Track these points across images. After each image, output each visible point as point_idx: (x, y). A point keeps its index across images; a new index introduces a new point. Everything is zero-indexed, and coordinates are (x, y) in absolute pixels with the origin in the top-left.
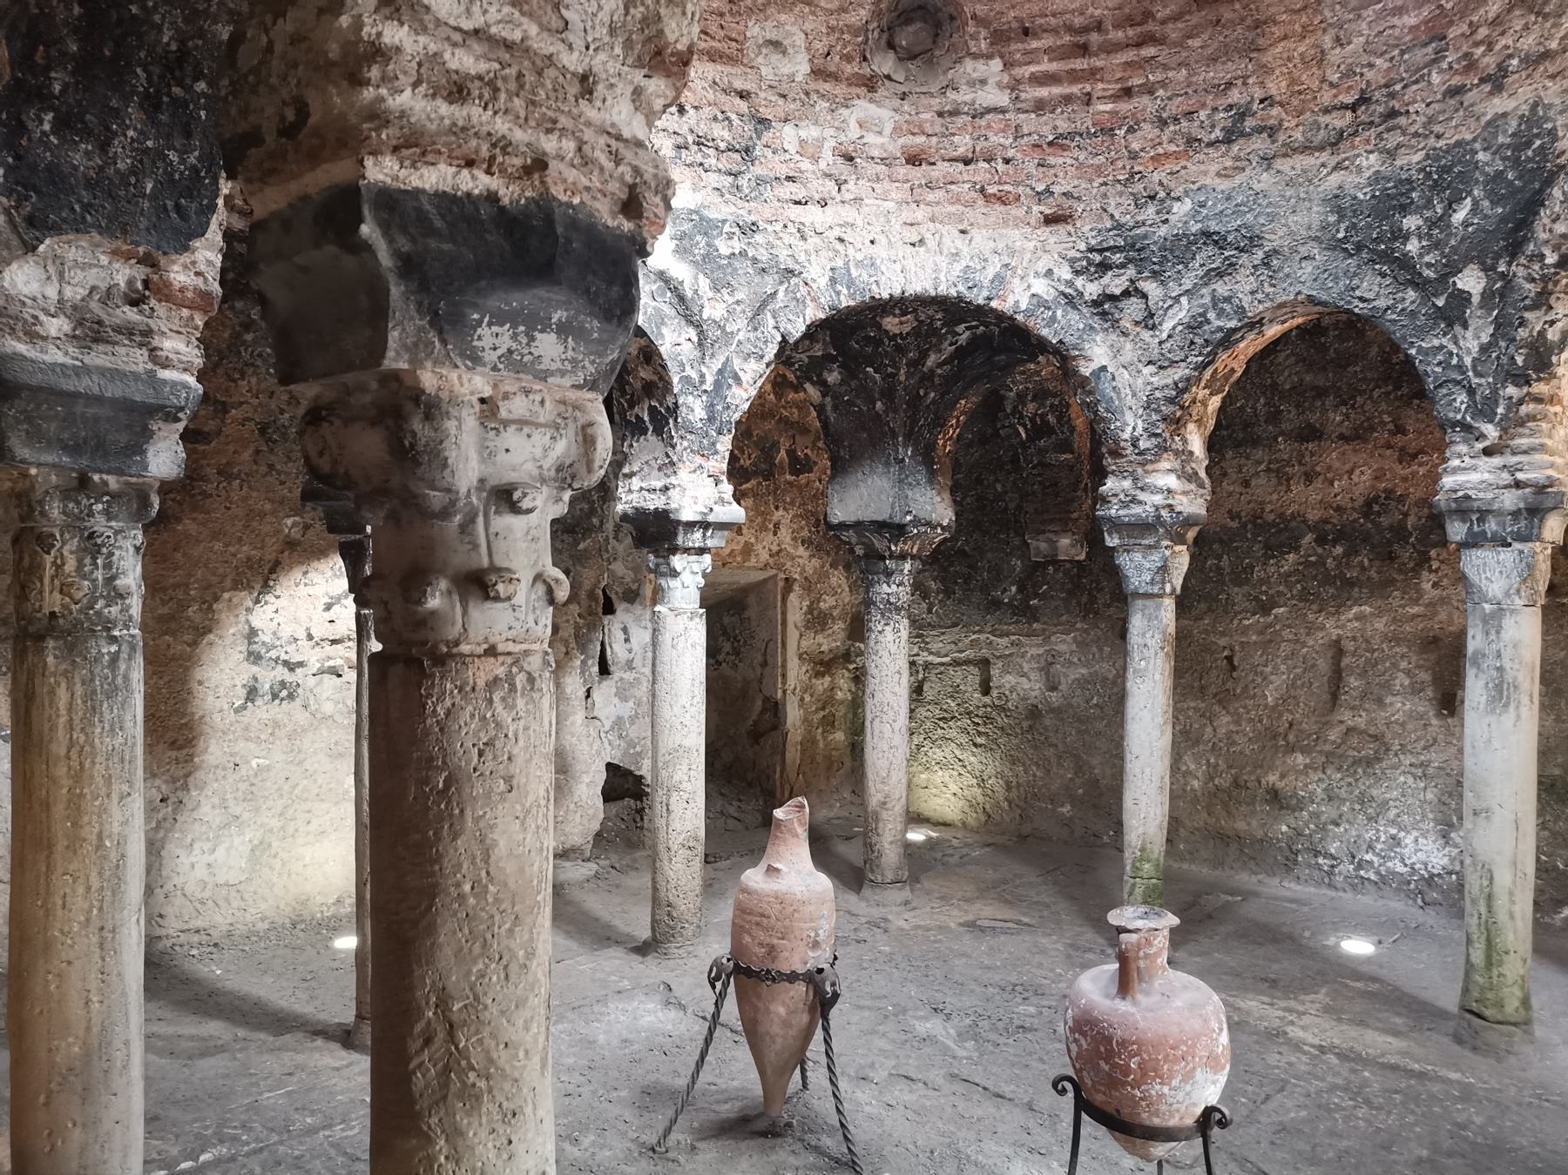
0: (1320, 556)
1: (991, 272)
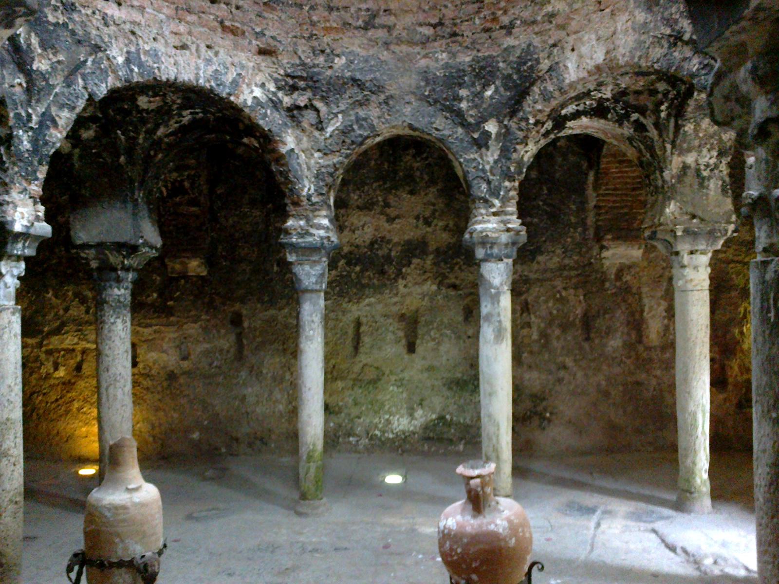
0: (348, 272)
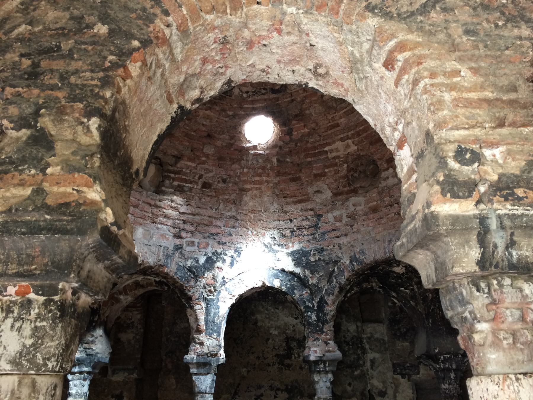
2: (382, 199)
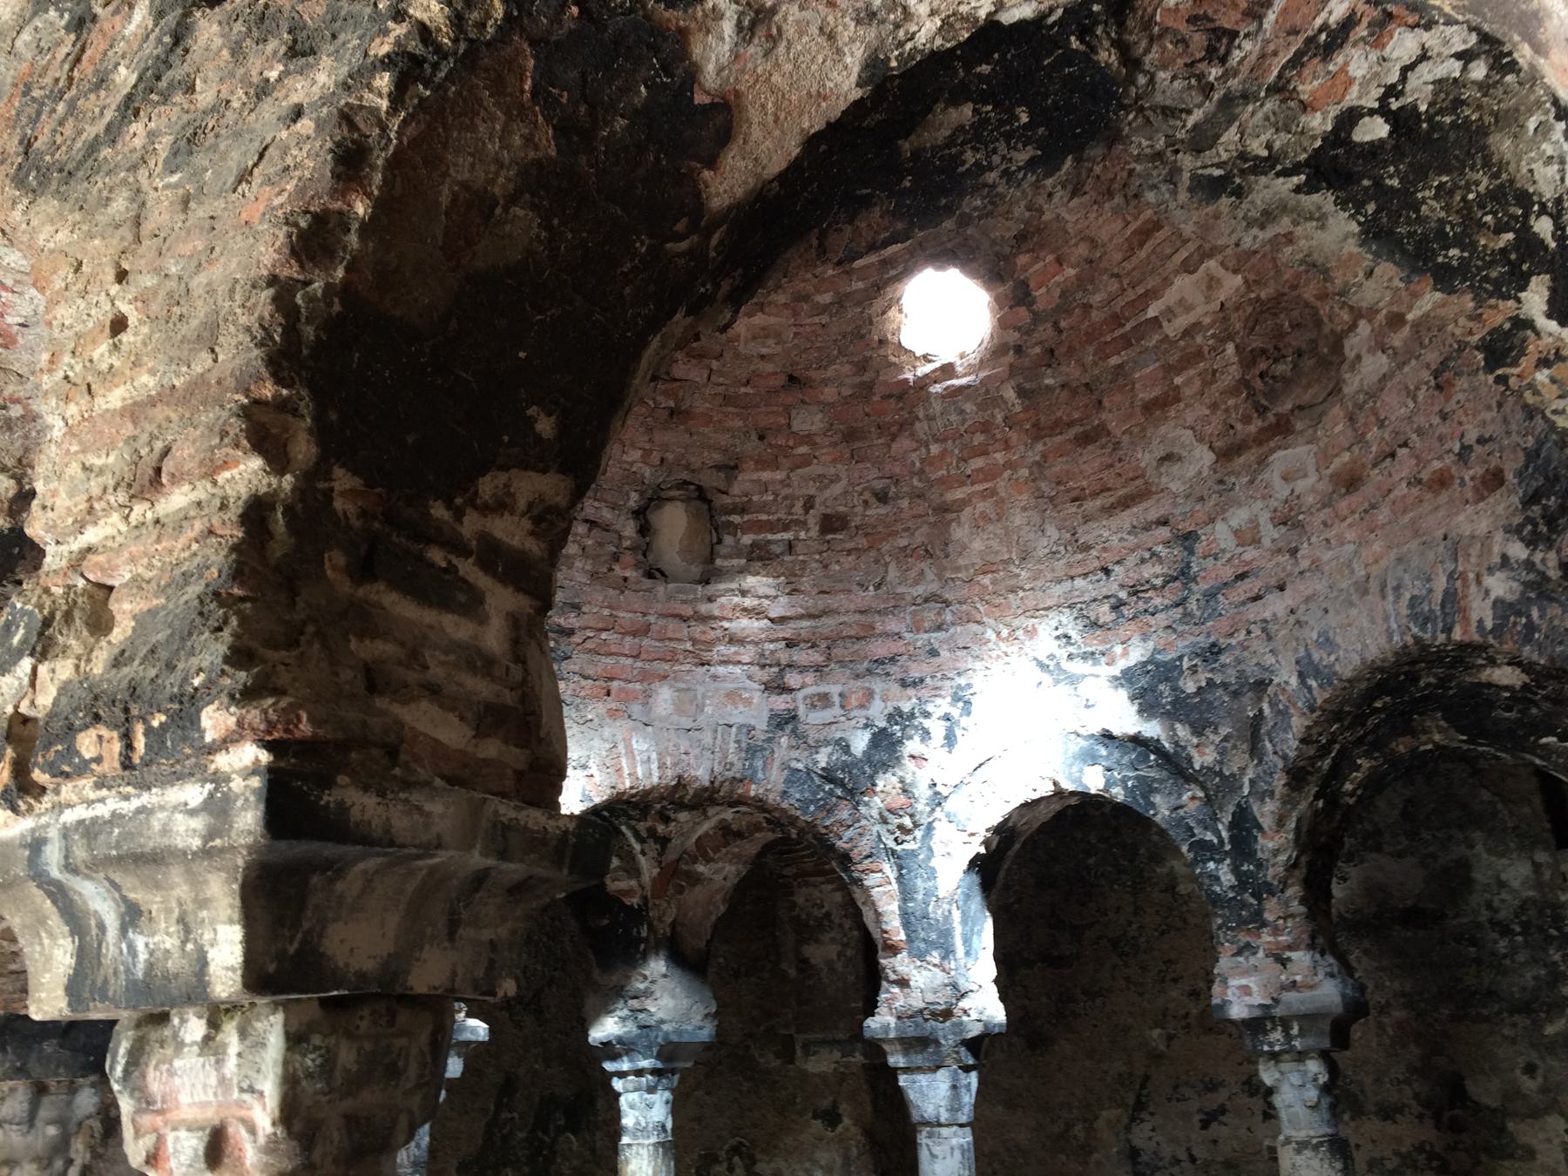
1: (1438, 596)
2: (1360, 439)
